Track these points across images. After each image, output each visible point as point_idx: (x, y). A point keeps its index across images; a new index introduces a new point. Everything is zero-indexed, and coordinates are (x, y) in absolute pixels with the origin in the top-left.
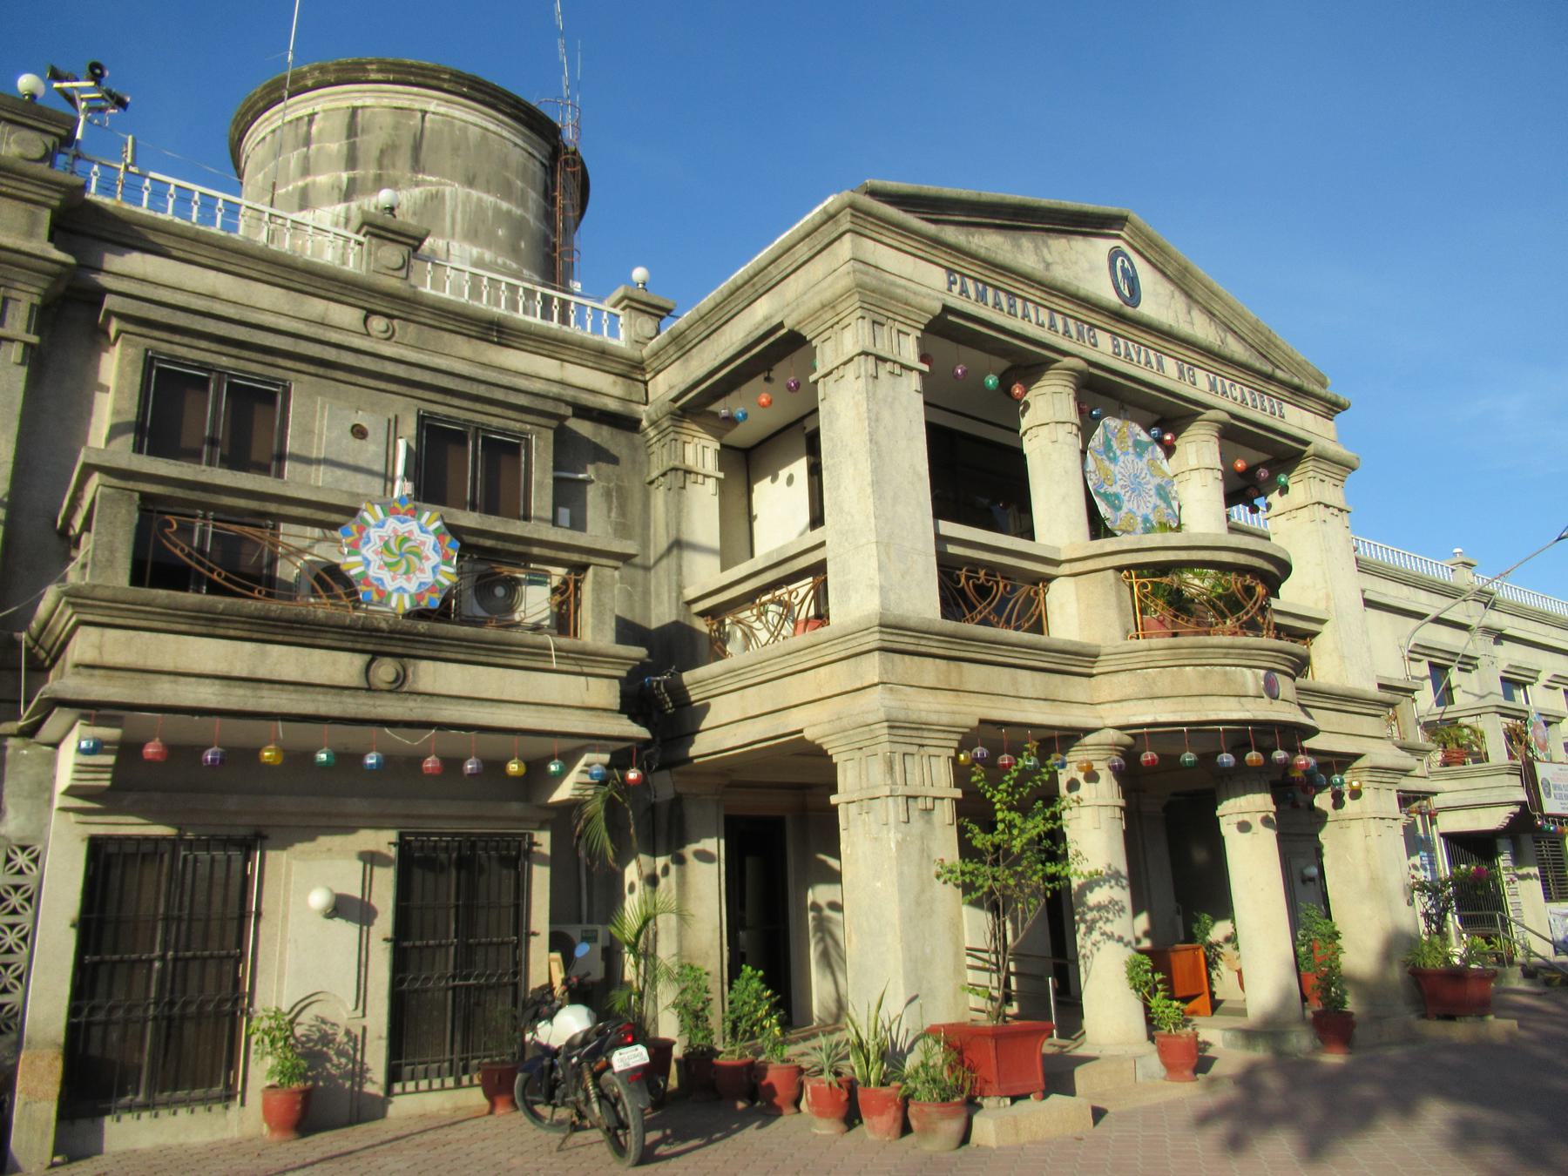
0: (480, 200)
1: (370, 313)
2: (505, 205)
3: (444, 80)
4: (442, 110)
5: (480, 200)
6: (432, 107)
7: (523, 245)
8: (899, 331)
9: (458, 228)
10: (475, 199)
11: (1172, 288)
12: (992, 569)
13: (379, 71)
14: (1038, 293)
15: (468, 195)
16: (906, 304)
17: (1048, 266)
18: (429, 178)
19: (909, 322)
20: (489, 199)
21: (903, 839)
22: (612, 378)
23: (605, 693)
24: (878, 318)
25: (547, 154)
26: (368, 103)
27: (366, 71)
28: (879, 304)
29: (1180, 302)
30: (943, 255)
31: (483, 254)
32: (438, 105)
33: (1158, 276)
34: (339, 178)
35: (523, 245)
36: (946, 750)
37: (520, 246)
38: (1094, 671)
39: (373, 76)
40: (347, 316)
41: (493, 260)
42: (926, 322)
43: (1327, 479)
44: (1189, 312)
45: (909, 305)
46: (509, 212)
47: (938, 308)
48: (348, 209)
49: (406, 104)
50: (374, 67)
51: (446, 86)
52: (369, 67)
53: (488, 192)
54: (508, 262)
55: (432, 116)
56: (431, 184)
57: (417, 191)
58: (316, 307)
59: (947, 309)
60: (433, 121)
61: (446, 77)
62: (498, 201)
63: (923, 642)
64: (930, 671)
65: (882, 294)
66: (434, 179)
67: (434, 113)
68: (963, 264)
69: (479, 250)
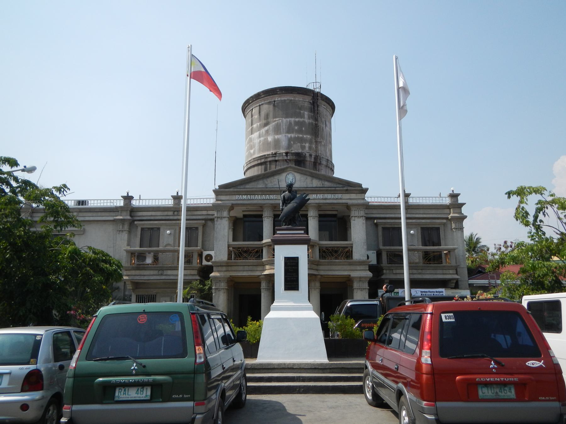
0: (290, 121)
1: (174, 211)
2: (297, 120)
3: (278, 91)
4: (279, 99)
5: (290, 121)
6: (276, 100)
7: (304, 129)
8: (223, 211)
9: (284, 131)
10: (288, 121)
11: (307, 176)
12: (247, 247)
13: (263, 94)
14: (260, 192)
15: (287, 121)
17: (266, 185)
18: (276, 119)
20: (292, 120)
23: (195, 272)
24: (218, 210)
25: (311, 99)
26: (263, 103)
27: (261, 95)
29: (309, 179)
31: (291, 135)
32: (278, 98)
33: (302, 175)
34: (258, 125)
35: (304, 129)
37: (302, 129)
38: (264, 264)
39: (262, 96)
40: (171, 213)
41: (294, 136)
44: (312, 181)
46: (299, 121)
47: (230, 205)
48: (260, 132)
49: (271, 100)
50: (262, 94)
51: (278, 93)
52: (261, 94)
53: (291, 118)
54: (299, 135)
55: (277, 102)
56: (277, 120)
57: (274, 123)
58: (166, 213)
59: (232, 204)
60: (277, 103)
61: (278, 90)
62: (295, 119)
64: (224, 269)
66: (278, 119)
67: (277, 101)
69: (290, 135)
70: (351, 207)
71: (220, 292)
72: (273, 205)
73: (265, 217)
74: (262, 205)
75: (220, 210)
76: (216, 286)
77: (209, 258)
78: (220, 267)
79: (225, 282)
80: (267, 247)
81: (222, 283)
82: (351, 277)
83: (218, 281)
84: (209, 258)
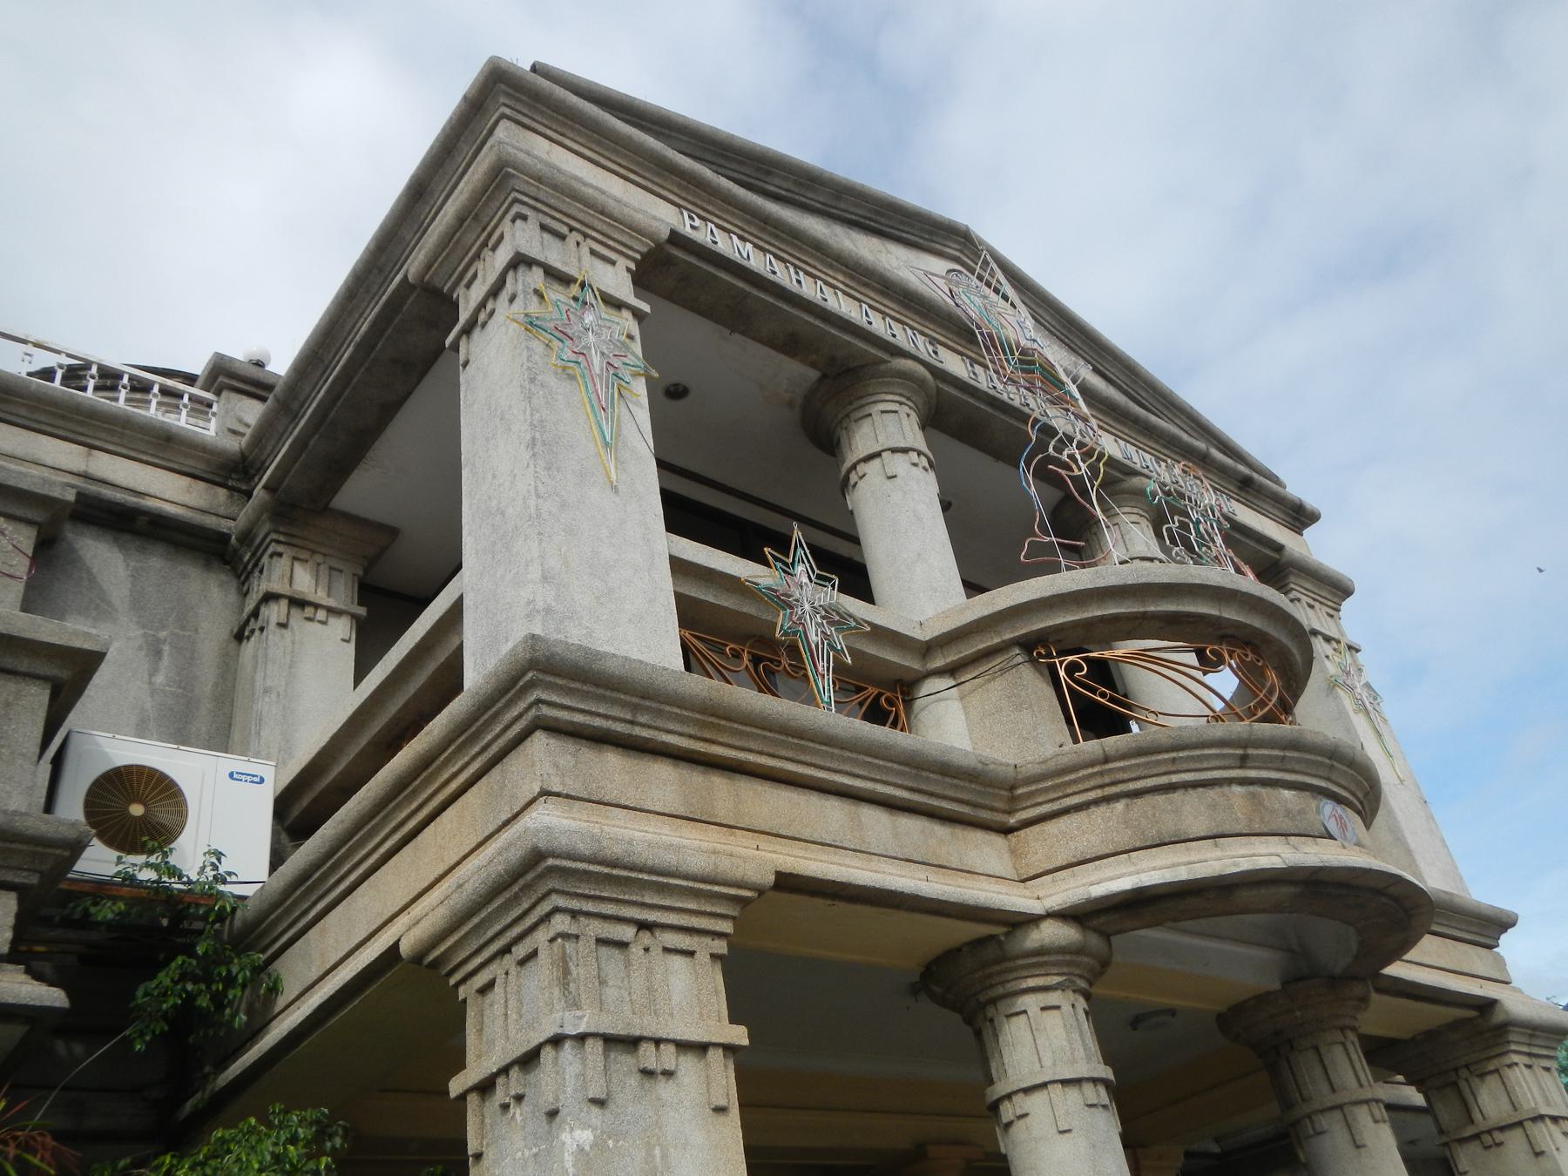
14: (840, 277)
16: (602, 213)
19: (611, 243)
21: (594, 1145)
22: (185, 481)
28: (552, 201)
30: (676, 190)
36: (708, 940)
38: (1012, 821)
42: (645, 250)
43: (1317, 605)
45: (610, 216)
63: (642, 719)
65: (555, 187)
68: (710, 208)
70: (1292, 579)
71: (664, 1089)
72: (946, 388)
73: (894, 450)
74: (880, 354)
75: (564, 230)
76: (611, 993)
77: (137, 810)
78: (613, 760)
79: (703, 957)
80: (1017, 655)
81: (678, 962)
82: (1498, 1018)
83: (627, 933)
84: (137, 810)
